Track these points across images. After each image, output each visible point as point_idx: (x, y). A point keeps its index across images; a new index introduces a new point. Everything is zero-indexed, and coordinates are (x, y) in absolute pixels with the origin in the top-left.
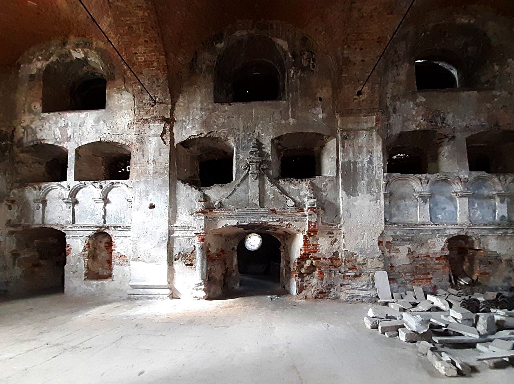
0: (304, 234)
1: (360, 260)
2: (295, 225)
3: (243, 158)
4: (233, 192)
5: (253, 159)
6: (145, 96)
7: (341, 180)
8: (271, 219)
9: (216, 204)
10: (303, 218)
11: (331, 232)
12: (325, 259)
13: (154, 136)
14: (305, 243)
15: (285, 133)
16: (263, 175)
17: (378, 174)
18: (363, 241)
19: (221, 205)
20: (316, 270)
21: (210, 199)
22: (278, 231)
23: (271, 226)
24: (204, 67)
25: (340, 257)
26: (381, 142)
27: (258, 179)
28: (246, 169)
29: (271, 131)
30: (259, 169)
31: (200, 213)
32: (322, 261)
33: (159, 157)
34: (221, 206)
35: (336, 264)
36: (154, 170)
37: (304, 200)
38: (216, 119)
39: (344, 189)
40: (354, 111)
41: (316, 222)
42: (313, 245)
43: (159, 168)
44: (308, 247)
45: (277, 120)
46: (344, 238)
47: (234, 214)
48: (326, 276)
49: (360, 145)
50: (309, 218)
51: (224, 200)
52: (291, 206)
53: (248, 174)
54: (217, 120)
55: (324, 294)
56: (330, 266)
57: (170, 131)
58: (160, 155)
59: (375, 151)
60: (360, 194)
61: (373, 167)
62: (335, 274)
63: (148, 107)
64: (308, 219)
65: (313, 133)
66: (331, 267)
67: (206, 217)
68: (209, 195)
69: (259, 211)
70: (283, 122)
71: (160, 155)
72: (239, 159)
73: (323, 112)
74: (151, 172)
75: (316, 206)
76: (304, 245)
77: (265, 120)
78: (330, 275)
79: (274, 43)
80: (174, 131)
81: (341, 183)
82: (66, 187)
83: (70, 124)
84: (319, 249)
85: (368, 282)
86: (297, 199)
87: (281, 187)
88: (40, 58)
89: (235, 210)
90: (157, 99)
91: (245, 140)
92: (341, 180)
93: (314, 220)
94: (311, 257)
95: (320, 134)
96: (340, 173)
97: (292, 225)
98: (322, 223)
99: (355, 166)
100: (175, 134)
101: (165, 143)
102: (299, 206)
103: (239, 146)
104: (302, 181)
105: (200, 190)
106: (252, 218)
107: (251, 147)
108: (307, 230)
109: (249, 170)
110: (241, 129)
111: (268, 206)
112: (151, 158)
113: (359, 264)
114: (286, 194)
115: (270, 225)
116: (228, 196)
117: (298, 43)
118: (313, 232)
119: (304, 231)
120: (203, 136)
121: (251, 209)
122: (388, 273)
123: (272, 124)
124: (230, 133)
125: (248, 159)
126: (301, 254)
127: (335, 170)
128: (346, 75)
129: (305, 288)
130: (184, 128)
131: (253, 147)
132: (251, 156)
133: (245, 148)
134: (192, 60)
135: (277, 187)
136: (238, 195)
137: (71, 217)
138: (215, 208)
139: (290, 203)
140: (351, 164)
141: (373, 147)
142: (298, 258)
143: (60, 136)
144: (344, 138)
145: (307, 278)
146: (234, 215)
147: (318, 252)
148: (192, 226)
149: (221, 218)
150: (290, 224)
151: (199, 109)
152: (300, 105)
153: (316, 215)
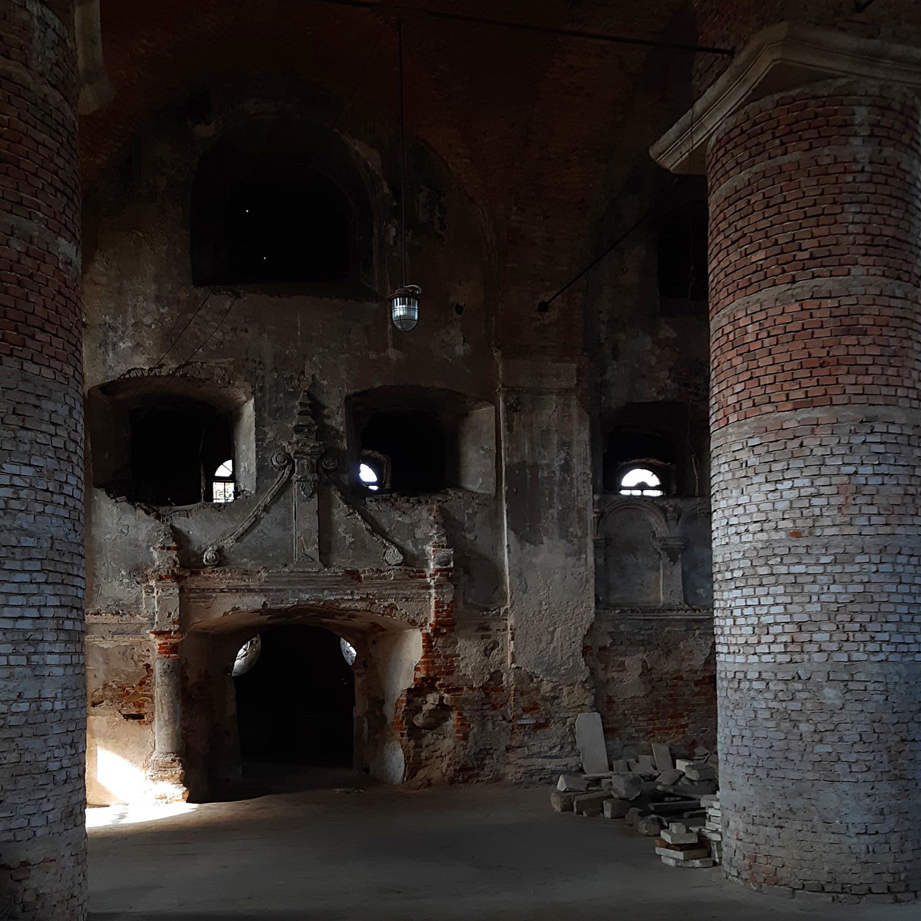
0: (425, 631)
4: (252, 527)
5: (305, 445)
8: (347, 594)
9: (208, 555)
10: (422, 591)
14: (426, 652)
17: (581, 496)
18: (552, 646)
19: (221, 559)
20: (449, 716)
21: (189, 541)
26: (587, 424)
27: (316, 495)
28: (284, 467)
31: (169, 581)
32: (466, 693)
34: (220, 561)
35: (496, 699)
37: (424, 551)
44: (433, 661)
46: (513, 639)
47: (258, 583)
48: (475, 728)
49: (544, 428)
50: (436, 593)
52: (396, 565)
56: (484, 704)
64: (434, 595)
66: (485, 707)
67: (181, 590)
84: (458, 666)
85: (563, 738)
86: (409, 546)
89: (259, 572)
97: (397, 609)
98: (465, 603)
106: (300, 590)
108: (432, 620)
109: (292, 472)
111: (341, 563)
113: (544, 699)
114: (384, 535)
119: (426, 622)
122: (602, 717)
126: (415, 679)
135: (362, 518)
136: (265, 533)
138: (205, 566)
139: (393, 556)
140: (528, 471)
142: (409, 690)
145: (429, 738)
146: (253, 584)
149: (222, 591)
150: (392, 607)
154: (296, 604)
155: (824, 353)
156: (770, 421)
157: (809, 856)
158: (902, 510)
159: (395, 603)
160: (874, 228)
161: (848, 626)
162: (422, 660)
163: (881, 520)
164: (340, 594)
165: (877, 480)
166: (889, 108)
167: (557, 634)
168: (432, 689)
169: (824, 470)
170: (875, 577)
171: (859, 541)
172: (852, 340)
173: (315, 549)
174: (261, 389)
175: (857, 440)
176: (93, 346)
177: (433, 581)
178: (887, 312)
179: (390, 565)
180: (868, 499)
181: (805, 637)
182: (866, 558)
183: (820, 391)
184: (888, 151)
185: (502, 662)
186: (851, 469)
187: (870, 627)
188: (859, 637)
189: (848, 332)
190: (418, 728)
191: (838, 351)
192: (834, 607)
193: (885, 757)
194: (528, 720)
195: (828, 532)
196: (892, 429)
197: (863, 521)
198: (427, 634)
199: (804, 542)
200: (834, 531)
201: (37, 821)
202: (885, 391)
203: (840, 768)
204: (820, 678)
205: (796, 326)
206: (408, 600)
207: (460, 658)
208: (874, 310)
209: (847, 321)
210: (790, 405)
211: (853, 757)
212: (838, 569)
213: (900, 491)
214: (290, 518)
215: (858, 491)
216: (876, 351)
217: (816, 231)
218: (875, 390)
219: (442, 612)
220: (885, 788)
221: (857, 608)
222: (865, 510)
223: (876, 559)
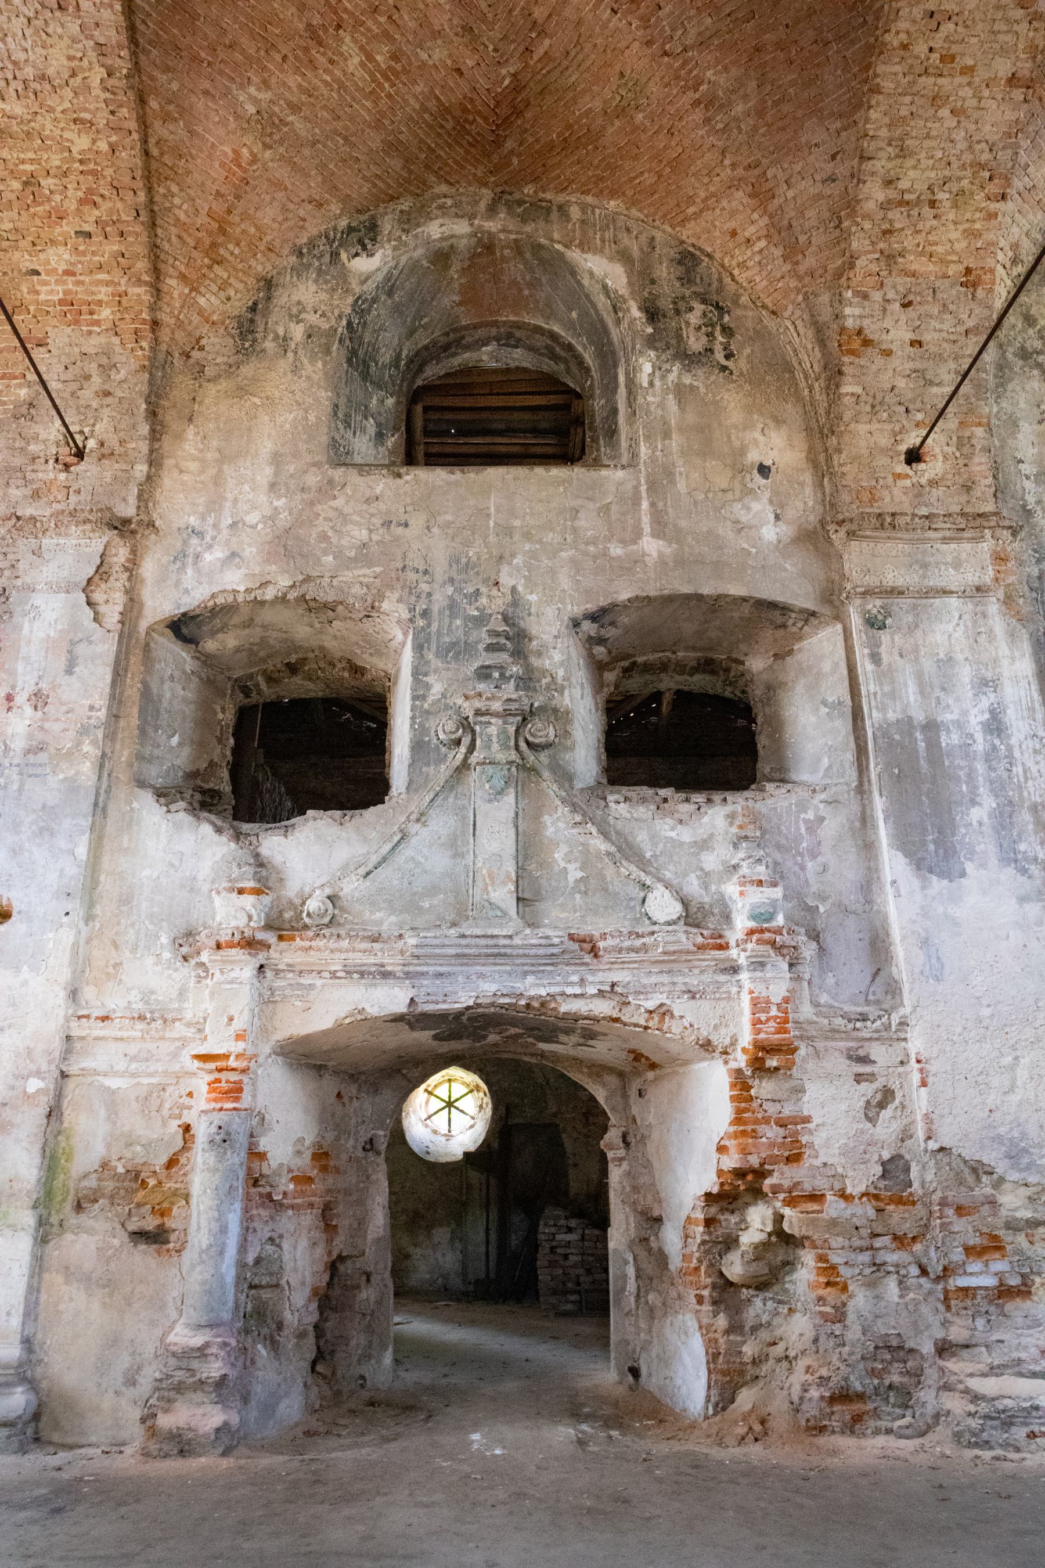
0: (733, 1065)
3: (444, 696)
6: (38, 428)
9: (313, 905)
10: (722, 978)
11: (861, 1053)
12: (843, 1195)
13: (54, 588)
14: (739, 1111)
15: (624, 596)
17: (1034, 779)
23: (576, 1018)
24: (298, 332)
25: (916, 1185)
26: (1026, 647)
28: (458, 742)
29: (565, 582)
30: (517, 747)
33: (63, 680)
36: (30, 736)
37: (722, 895)
38: (332, 528)
40: (901, 521)
41: (786, 1000)
42: (782, 1124)
43: (56, 727)
45: (594, 541)
46: (924, 1084)
49: (942, 656)
50: (753, 980)
52: (668, 923)
53: (465, 766)
55: (857, 1407)
56: (875, 1235)
57: (127, 569)
58: (69, 671)
59: (1006, 682)
60: (969, 867)
61: (1010, 749)
62: (900, 1283)
63: (50, 473)
64: (747, 985)
65: (744, 599)
66: (878, 1243)
68: (278, 859)
69: (517, 941)
70: (616, 550)
71: (69, 671)
72: (424, 698)
73: (777, 517)
74: (18, 745)
75: (780, 920)
76: (738, 1120)
77: (540, 542)
80: (148, 568)
81: (880, 816)
86: (693, 886)
87: (617, 833)
90: (91, 444)
91: (453, 616)
93: (778, 991)
94: (776, 1189)
95: (773, 605)
97: (672, 1016)
98: (816, 1005)
99: (933, 744)
100: (149, 582)
103: (428, 641)
104: (709, 801)
105: (238, 836)
106: (481, 976)
107: (481, 646)
108: (746, 1039)
109: (472, 748)
110: (440, 570)
112: (26, 683)
113: (1012, 1226)
114: (643, 864)
115: (567, 1016)
116: (370, 867)
119: (734, 1042)
120: (270, 594)
121: (478, 932)
123: (572, 561)
124: (391, 588)
125: (467, 698)
126: (720, 1173)
127: (850, 756)
128: (858, 390)
129: (751, 1371)
130: (190, 560)
131: (491, 648)
132: (481, 687)
134: (253, 309)
136: (418, 864)
138: (306, 927)
140: (919, 735)
141: (996, 661)
142: (708, 1196)
144: (875, 624)
145: (758, 1308)
146: (392, 962)
147: (807, 1162)
148: (188, 1015)
149: (334, 975)
150: (663, 1012)
151: (266, 487)
152: (682, 486)
153: (785, 966)
154: (471, 1003)
159: (668, 1002)
162: (732, 1129)
164: (557, 984)
167: (1022, 1074)
168: (757, 1194)
173: (510, 892)
176: (165, 560)
177: (743, 955)
179: (655, 923)
185: (906, 1135)
190: (731, 1284)
198: (739, 1071)
206: (693, 998)
207: (811, 1126)
214: (463, 833)
219: (768, 1020)
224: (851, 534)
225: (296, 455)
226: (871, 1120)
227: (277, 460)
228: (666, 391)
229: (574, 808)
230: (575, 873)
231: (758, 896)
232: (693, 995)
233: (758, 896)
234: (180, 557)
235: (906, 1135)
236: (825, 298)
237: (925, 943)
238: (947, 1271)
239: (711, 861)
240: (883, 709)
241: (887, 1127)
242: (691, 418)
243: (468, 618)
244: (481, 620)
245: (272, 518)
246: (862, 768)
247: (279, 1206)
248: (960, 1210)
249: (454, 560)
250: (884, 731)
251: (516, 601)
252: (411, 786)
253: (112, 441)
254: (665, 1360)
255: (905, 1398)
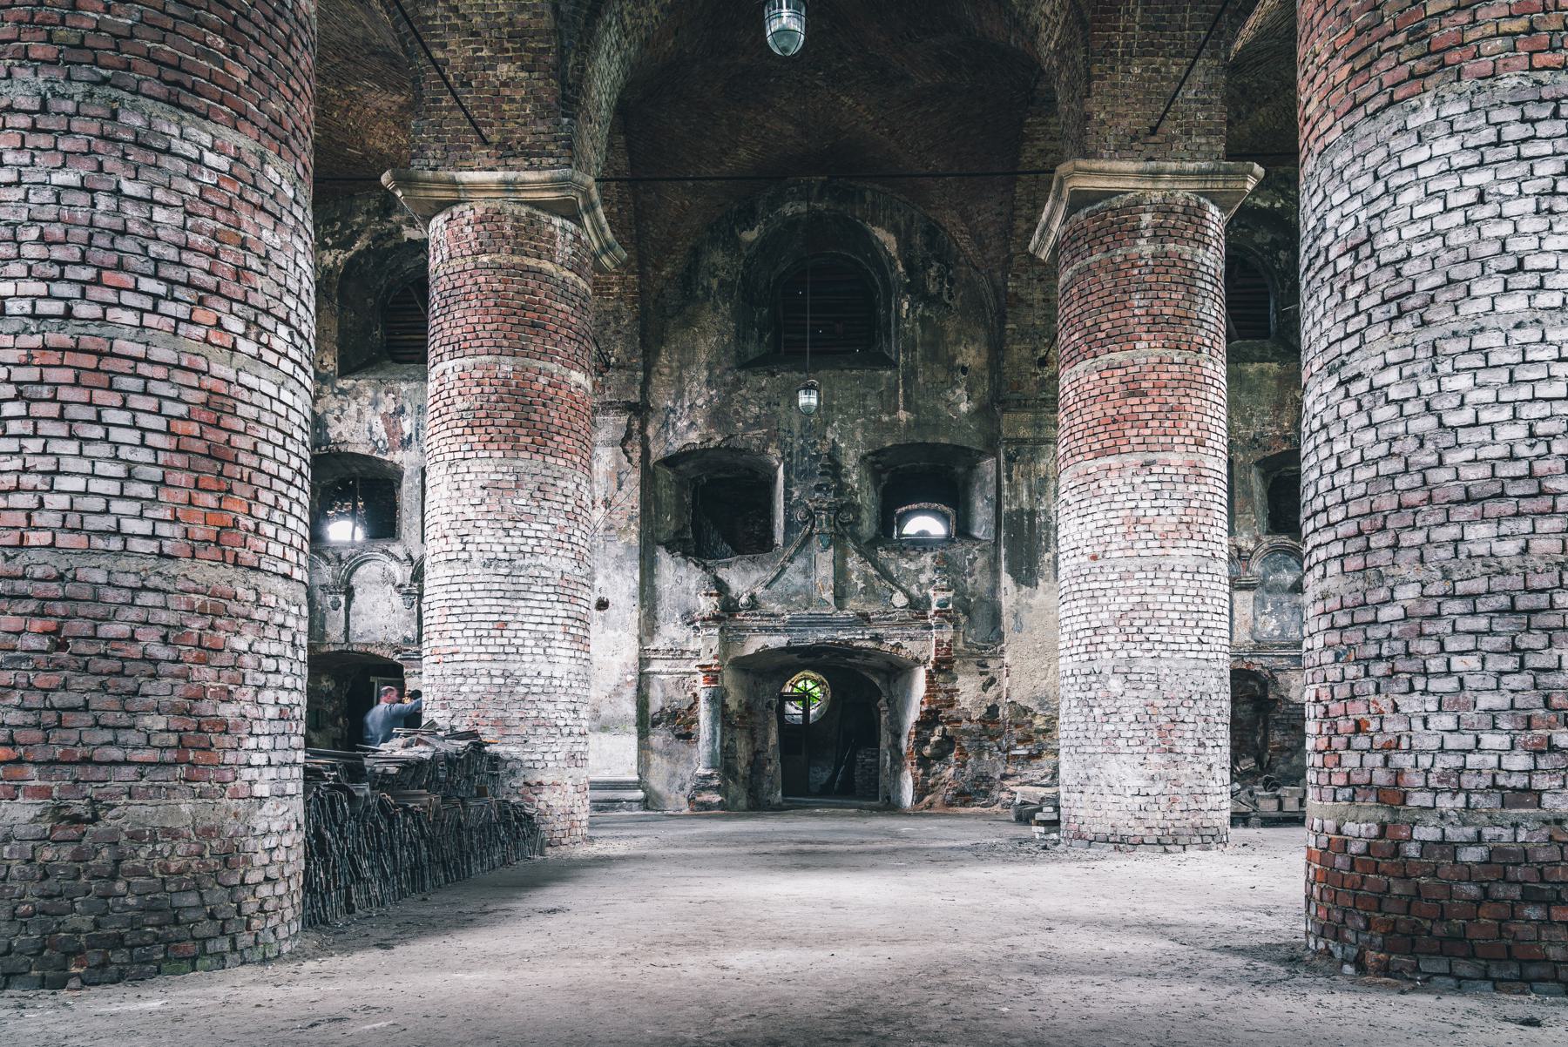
1: (1039, 722)
2: (911, 648)
4: (779, 576)
7: (1003, 551)
9: (743, 600)
12: (970, 720)
13: (607, 444)
15: (889, 444)
16: (843, 536)
19: (754, 602)
21: (728, 589)
22: (874, 661)
23: (860, 648)
24: (715, 283)
29: (859, 437)
32: (965, 725)
39: (1013, 572)
45: (874, 413)
51: (759, 591)
53: (810, 535)
54: (745, 410)
58: (619, 489)
60: (1040, 581)
67: (721, 630)
70: (885, 418)
71: (619, 489)
78: (979, 756)
79: (868, 235)
80: (650, 432)
82: (402, 556)
83: (408, 408)
86: (914, 590)
88: (328, 240)
92: (1003, 551)
93: (947, 637)
96: (1003, 535)
98: (965, 642)
99: (1032, 522)
101: (630, 460)
102: (917, 606)
105: (705, 568)
108: (932, 658)
110: (796, 430)
111: (853, 606)
112: (600, 494)
113: (1038, 731)
114: (892, 580)
117: (918, 240)
118: (944, 666)
120: (712, 445)
133: (807, 474)
134: (689, 269)
137: (414, 627)
139: (899, 600)
143: (384, 436)
144: (1010, 459)
150: (899, 646)
152: (920, 380)
155: (1114, 412)
156: (1081, 469)
157: (1098, 814)
158: (1176, 535)
160: (1156, 310)
161: (1129, 630)
163: (1157, 544)
165: (1155, 512)
166: (1172, 211)
168: (937, 722)
169: (1114, 506)
170: (1150, 591)
171: (1138, 561)
172: (1136, 400)
174: (790, 455)
175: (1138, 480)
178: (1165, 376)
180: (1145, 528)
181: (1097, 639)
182: (1143, 575)
183: (1111, 442)
184: (1171, 246)
185: (999, 696)
186: (1133, 504)
187: (1145, 630)
188: (1137, 638)
189: (1133, 394)
191: (1125, 410)
192: (1118, 615)
193: (1155, 735)
194: (1021, 751)
195: (1115, 554)
196: (1167, 470)
197: (1141, 545)
199: (1099, 563)
200: (1120, 553)
201: (549, 757)
202: (1162, 439)
203: (1121, 743)
204: (1107, 671)
205: (1096, 392)
208: (1154, 376)
209: (1132, 386)
210: (1091, 455)
211: (1130, 734)
212: (1121, 584)
213: (1175, 520)
215: (1138, 521)
216: (1155, 408)
217: (1111, 316)
218: (1154, 440)
220: (1155, 758)
221: (1136, 615)
222: (1143, 536)
223: (1151, 575)
224: (1004, 411)
225: (719, 363)
226: (985, 691)
227: (710, 367)
228: (915, 320)
229: (861, 554)
230: (861, 585)
231: (941, 596)
232: (911, 639)
233: (941, 596)
234: (665, 424)
235: (999, 696)
236: (999, 274)
237: (1016, 616)
238: (1010, 748)
239: (923, 579)
240: (1010, 504)
241: (991, 693)
242: (928, 337)
243: (811, 457)
244: (817, 458)
245: (711, 401)
246: (998, 534)
247: (734, 727)
248: (1017, 726)
249: (803, 425)
250: (1010, 514)
251: (835, 447)
252: (786, 544)
253: (624, 357)
254: (899, 791)
255: (986, 794)
